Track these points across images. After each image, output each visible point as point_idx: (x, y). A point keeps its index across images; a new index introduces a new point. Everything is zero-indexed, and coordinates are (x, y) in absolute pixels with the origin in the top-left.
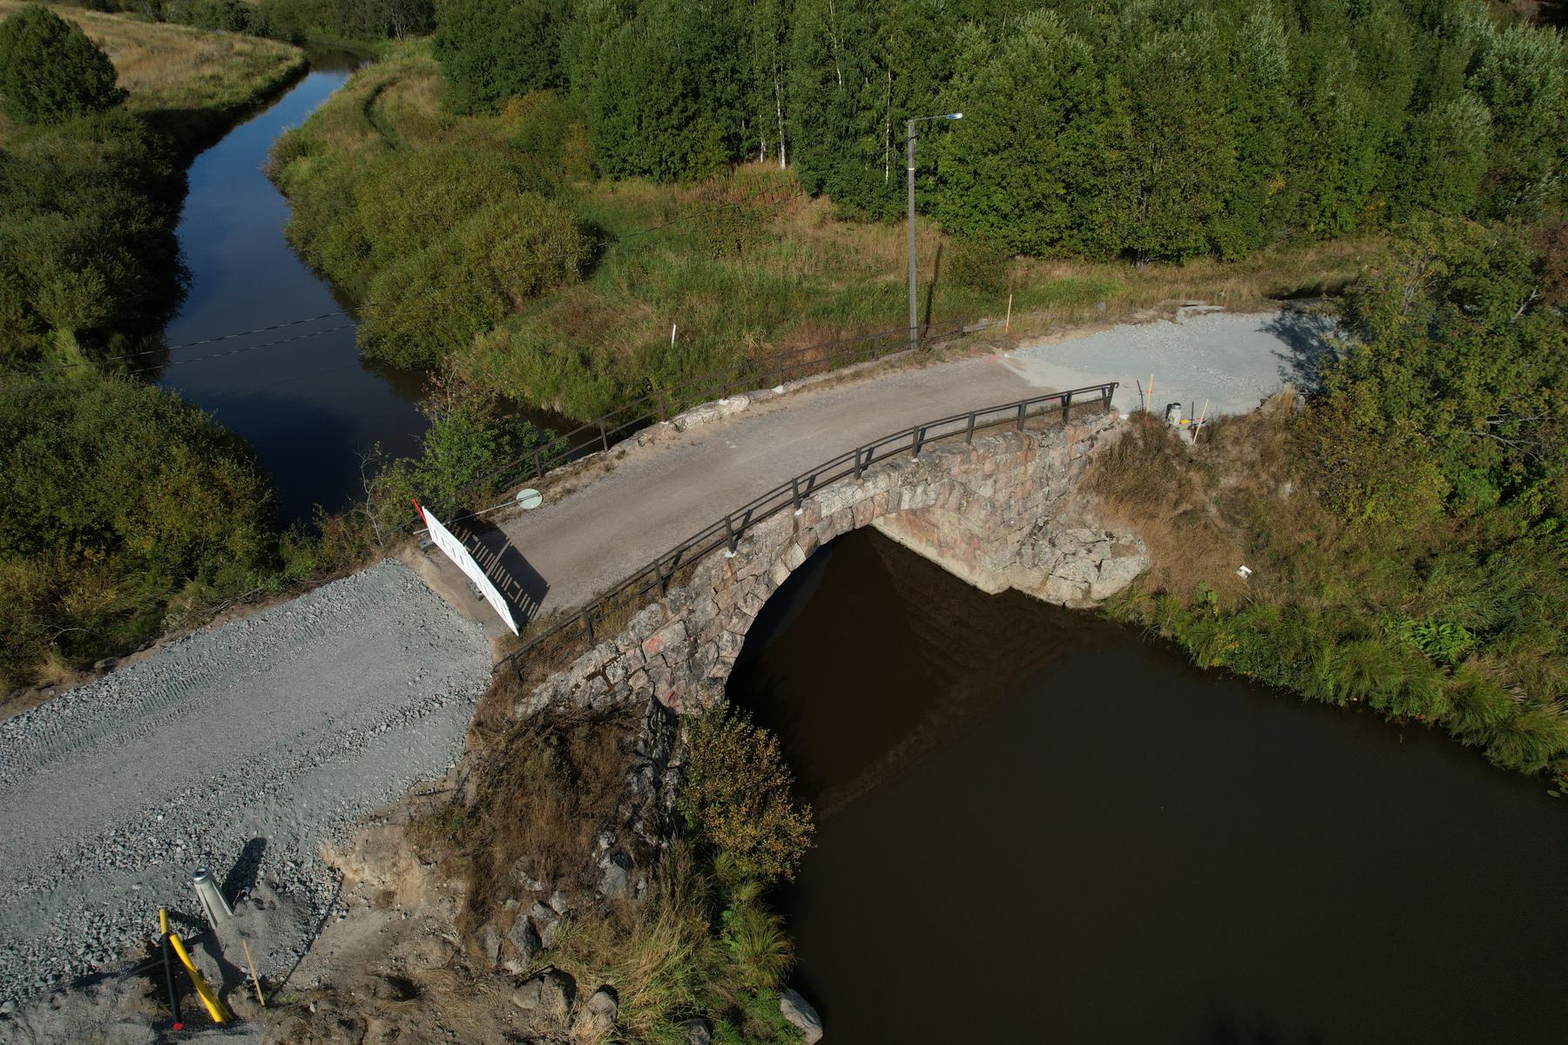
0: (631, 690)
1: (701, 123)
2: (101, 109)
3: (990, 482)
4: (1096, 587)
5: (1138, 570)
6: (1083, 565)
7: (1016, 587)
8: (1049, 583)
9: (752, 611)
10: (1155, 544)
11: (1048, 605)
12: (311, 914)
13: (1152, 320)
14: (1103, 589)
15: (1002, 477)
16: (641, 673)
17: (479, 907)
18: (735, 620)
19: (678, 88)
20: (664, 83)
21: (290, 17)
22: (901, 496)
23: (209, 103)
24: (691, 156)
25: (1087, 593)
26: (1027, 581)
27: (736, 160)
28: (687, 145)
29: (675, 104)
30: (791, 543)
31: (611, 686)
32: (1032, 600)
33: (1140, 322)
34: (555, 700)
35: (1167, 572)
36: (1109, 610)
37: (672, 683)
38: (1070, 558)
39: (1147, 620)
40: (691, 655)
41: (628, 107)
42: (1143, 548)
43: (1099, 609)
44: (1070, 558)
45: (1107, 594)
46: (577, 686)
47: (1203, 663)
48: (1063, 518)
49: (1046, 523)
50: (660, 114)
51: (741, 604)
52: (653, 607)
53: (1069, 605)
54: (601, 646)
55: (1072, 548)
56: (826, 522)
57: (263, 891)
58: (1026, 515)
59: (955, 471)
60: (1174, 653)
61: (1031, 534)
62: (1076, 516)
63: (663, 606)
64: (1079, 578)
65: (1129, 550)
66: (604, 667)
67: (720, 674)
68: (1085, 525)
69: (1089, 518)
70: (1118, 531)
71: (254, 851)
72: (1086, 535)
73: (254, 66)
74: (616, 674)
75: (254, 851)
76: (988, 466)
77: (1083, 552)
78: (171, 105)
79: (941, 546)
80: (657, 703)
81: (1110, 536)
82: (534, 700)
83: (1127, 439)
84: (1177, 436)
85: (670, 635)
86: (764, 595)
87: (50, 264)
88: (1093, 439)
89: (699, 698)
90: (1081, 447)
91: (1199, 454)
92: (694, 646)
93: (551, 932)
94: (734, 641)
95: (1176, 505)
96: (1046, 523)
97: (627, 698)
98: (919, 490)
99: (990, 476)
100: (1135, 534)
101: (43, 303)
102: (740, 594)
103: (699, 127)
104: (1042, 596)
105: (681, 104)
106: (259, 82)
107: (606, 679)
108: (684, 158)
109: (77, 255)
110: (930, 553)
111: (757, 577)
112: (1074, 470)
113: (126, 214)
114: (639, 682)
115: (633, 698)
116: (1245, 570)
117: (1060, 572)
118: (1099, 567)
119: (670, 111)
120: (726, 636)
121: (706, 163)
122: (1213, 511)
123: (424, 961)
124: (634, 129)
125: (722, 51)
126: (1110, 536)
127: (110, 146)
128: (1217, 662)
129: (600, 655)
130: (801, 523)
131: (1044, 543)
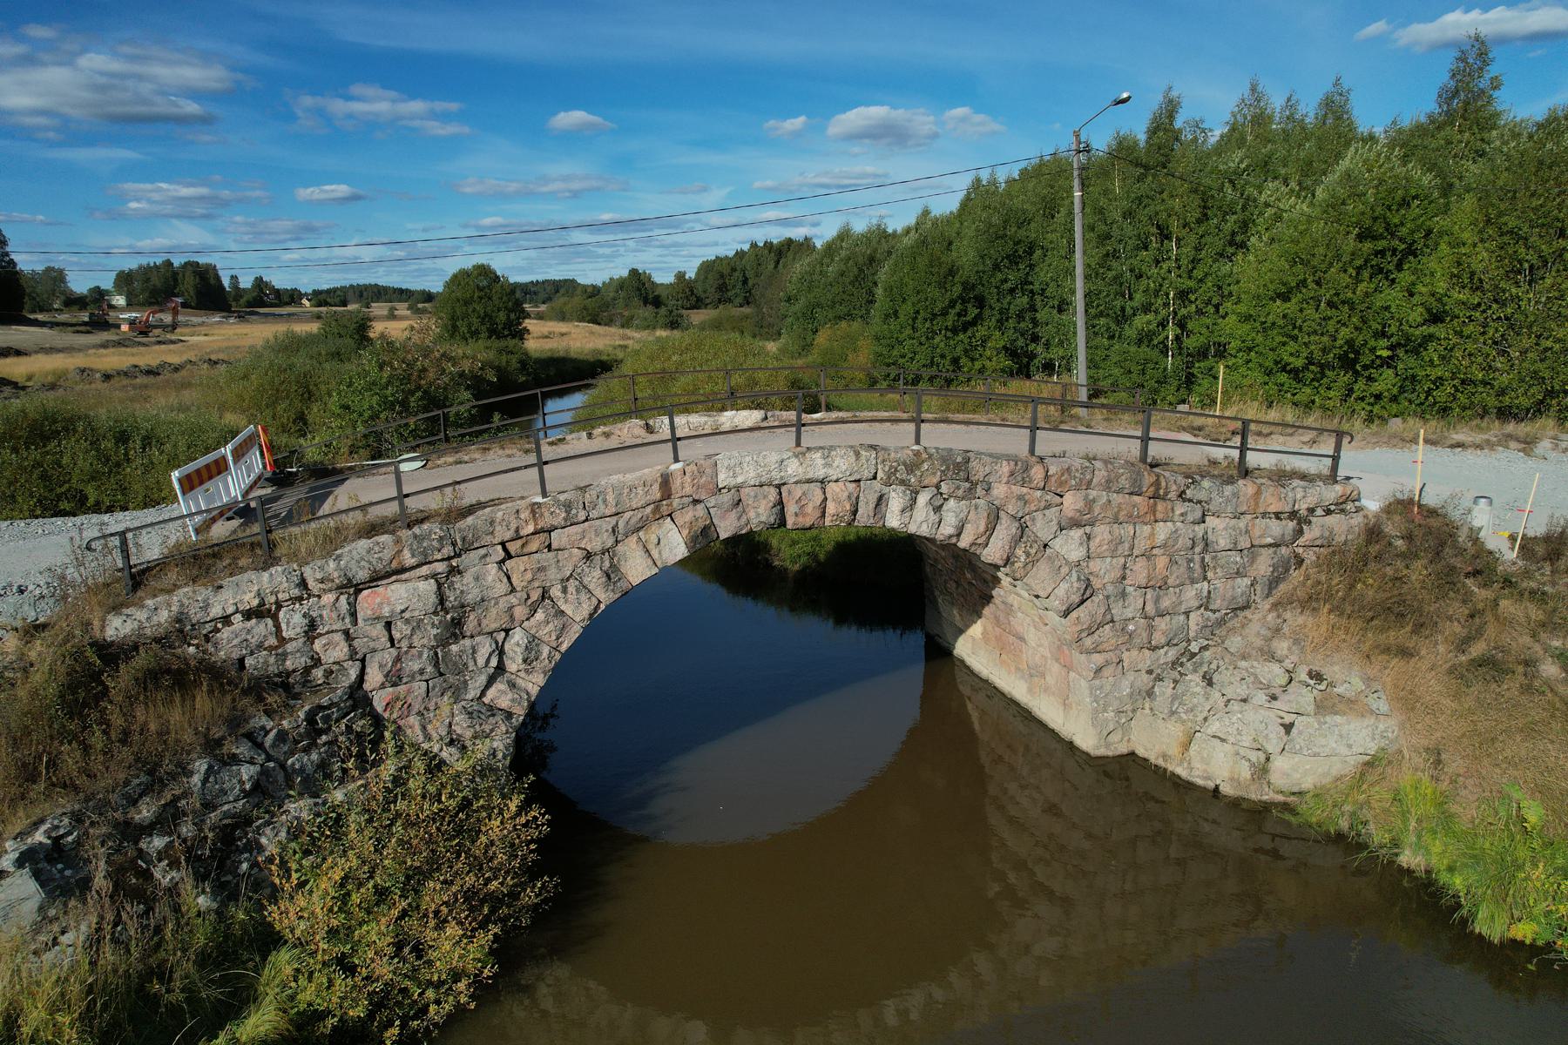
0: (317, 662)
1: (981, 331)
3: (1077, 534)
4: (1279, 764)
5: (1372, 748)
6: (1259, 721)
7: (1141, 752)
8: (1194, 747)
9: (578, 611)
10: (1407, 701)
11: (1189, 786)
13: (1490, 445)
15: (1102, 532)
16: (338, 637)
18: (540, 615)
20: (942, 285)
22: (881, 500)
24: (963, 361)
25: (1262, 771)
26: (1154, 739)
27: (1024, 372)
29: (952, 304)
30: (658, 515)
31: (283, 641)
32: (1160, 774)
33: (1460, 445)
34: (181, 630)
36: (1303, 808)
37: (394, 678)
38: (1235, 706)
39: (1377, 835)
40: (443, 642)
41: (906, 310)
42: (1384, 707)
43: (1286, 807)
44: (1235, 706)
45: (1307, 784)
46: (226, 620)
47: (1491, 924)
48: (1235, 643)
49: (1204, 648)
50: (934, 316)
51: (556, 592)
52: (385, 538)
53: (1226, 789)
54: (277, 570)
55: (1242, 691)
56: (726, 498)
58: (1162, 624)
59: (999, 490)
60: (1428, 907)
61: (1175, 664)
62: (1259, 642)
63: (398, 541)
64: (1246, 741)
65: (1350, 705)
66: (279, 606)
67: (504, 703)
68: (1272, 657)
69: (1282, 647)
70: (1333, 671)
72: (1274, 673)
74: (293, 621)
77: (1261, 698)
78: (573, 355)
79: (1034, 674)
80: (358, 697)
81: (1317, 676)
82: (141, 615)
83: (1373, 533)
84: (1476, 541)
85: (409, 595)
86: (606, 597)
88: (1301, 520)
89: (460, 727)
90: (1277, 529)
91: (1527, 574)
92: (455, 629)
94: (550, 658)
95: (1463, 644)
96: (1204, 648)
97: (307, 670)
98: (923, 499)
99: (1076, 524)
100: (1368, 680)
102: (553, 575)
103: (978, 335)
104: (1181, 771)
105: (958, 307)
107: (278, 626)
108: (955, 361)
110: (1017, 688)
111: (589, 556)
112: (1263, 566)
114: (333, 651)
115: (318, 673)
117: (1214, 727)
118: (1288, 728)
119: (944, 313)
120: (518, 636)
121: (981, 371)
124: (909, 331)
125: (1013, 259)
126: (1317, 676)
128: (1525, 931)
129: (273, 581)
130: (676, 484)
131: (1194, 681)
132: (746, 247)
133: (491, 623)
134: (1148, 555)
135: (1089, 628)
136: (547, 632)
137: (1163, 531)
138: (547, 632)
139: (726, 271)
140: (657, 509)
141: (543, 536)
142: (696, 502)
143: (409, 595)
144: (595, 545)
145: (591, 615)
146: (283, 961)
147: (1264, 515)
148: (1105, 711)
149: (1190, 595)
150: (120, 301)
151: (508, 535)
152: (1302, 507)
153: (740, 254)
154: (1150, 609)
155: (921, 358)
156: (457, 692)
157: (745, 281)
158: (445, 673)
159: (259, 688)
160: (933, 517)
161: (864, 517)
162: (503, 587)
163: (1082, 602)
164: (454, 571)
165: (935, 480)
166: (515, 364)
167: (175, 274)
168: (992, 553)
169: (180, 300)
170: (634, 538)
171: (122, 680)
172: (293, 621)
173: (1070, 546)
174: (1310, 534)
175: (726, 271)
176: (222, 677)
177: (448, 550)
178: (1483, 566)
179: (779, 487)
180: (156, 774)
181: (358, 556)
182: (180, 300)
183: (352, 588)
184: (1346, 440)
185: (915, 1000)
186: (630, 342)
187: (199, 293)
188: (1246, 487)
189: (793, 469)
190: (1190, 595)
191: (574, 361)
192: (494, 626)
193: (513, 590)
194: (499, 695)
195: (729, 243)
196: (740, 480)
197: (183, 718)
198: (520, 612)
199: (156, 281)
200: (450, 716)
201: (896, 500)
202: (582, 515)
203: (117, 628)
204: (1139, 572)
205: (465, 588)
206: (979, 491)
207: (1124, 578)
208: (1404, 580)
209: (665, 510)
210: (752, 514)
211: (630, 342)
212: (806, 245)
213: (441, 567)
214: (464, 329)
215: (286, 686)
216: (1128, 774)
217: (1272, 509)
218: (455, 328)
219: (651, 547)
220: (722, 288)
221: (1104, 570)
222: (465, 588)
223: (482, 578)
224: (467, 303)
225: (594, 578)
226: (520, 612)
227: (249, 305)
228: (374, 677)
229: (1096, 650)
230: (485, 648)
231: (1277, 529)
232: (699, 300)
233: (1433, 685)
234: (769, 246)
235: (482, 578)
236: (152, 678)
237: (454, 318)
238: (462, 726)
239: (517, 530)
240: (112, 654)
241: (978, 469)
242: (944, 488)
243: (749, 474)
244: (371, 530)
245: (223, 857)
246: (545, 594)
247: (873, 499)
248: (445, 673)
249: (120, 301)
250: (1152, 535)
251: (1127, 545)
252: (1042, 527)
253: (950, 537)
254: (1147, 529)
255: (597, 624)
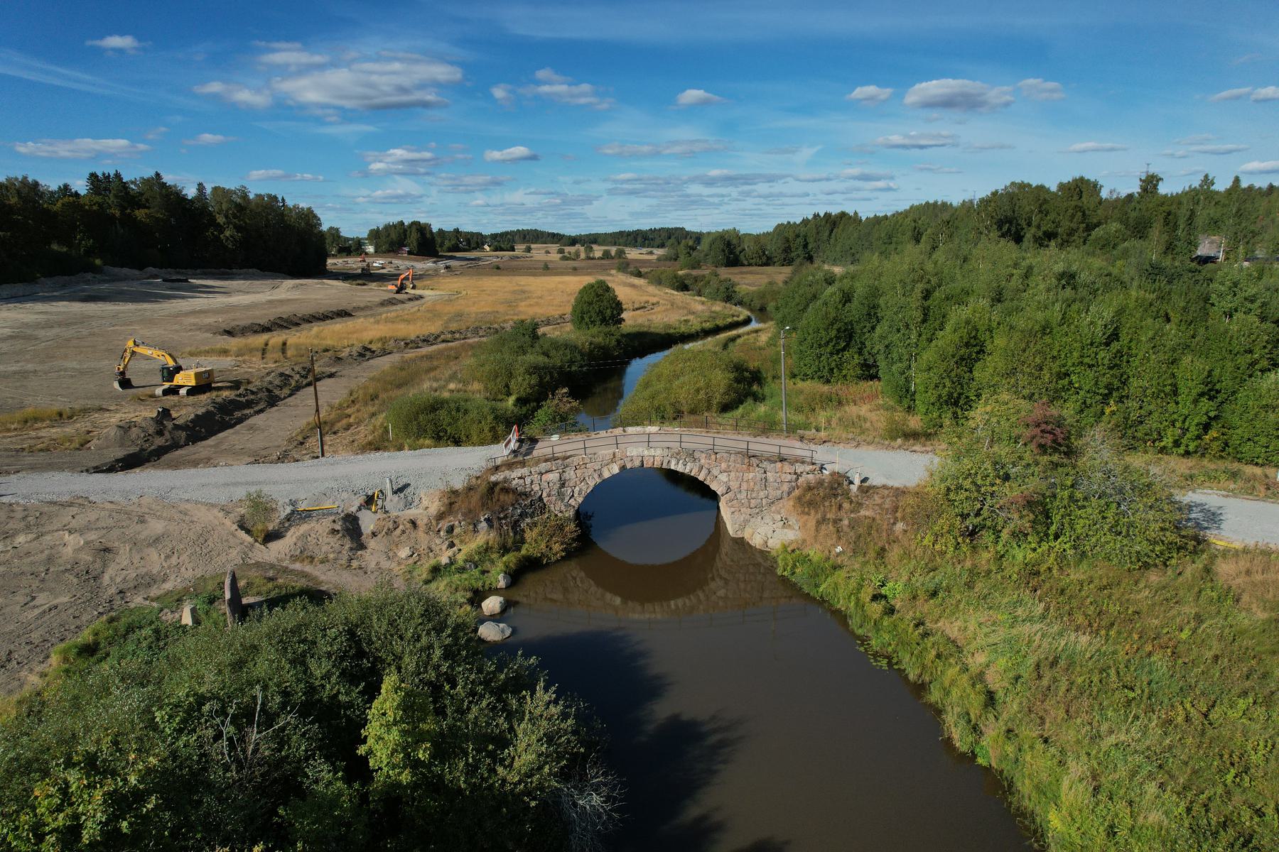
2: (607, 324)
9: (592, 484)
10: (803, 527)
12: (408, 505)
14: (775, 544)
15: (733, 474)
17: (440, 517)
19: (833, 333)
20: (826, 330)
21: (762, 295)
23: (672, 331)
28: (833, 364)
29: (831, 340)
34: (506, 480)
35: (804, 541)
37: (549, 495)
57: (402, 495)
71: (407, 486)
73: (714, 316)
74: (528, 481)
75: (407, 486)
76: (724, 465)
78: (652, 330)
80: (541, 499)
83: (820, 483)
85: (553, 476)
86: (599, 481)
87: (522, 370)
88: (798, 475)
89: (563, 509)
90: (789, 477)
92: (563, 485)
93: (457, 531)
101: (513, 385)
106: (707, 325)
108: (832, 370)
109: (534, 369)
112: (786, 487)
113: (572, 362)
114: (536, 488)
116: (839, 549)
122: (846, 522)
123: (421, 523)
127: (599, 340)
129: (525, 471)
132: (810, 217)
134: (748, 481)
136: (584, 488)
137: (751, 475)
138: (584, 488)
139: (791, 236)
143: (553, 476)
146: (526, 546)
149: (762, 494)
150: (371, 249)
152: (799, 471)
153: (805, 222)
155: (814, 368)
156: (562, 500)
157: (806, 246)
158: (560, 495)
159: (521, 494)
161: (665, 466)
166: (614, 343)
167: (405, 231)
168: (701, 478)
169: (407, 249)
171: (497, 489)
172: (528, 481)
173: (723, 477)
174: (801, 480)
175: (791, 236)
176: (514, 491)
178: (846, 494)
180: (503, 509)
181: (543, 466)
182: (407, 249)
183: (542, 474)
185: (680, 602)
186: (691, 317)
187: (420, 245)
188: (779, 465)
189: (646, 453)
190: (762, 494)
194: (572, 502)
195: (797, 213)
197: (509, 498)
199: (394, 236)
200: (560, 506)
203: (493, 478)
204: (744, 486)
205: (566, 476)
208: (826, 495)
211: (691, 317)
212: (855, 219)
214: (587, 320)
215: (526, 495)
216: (741, 543)
218: (583, 318)
220: (787, 250)
221: (734, 485)
222: (566, 476)
223: (570, 474)
224: (590, 304)
225: (596, 476)
227: (450, 250)
228: (544, 495)
231: (789, 477)
232: (769, 258)
233: (811, 521)
234: (827, 215)
235: (570, 474)
236: (502, 489)
237: (583, 313)
238: (563, 508)
240: (496, 484)
241: (697, 455)
243: (634, 453)
244: (546, 461)
245: (515, 525)
248: (560, 495)
249: (371, 249)
252: (715, 472)
255: (596, 487)
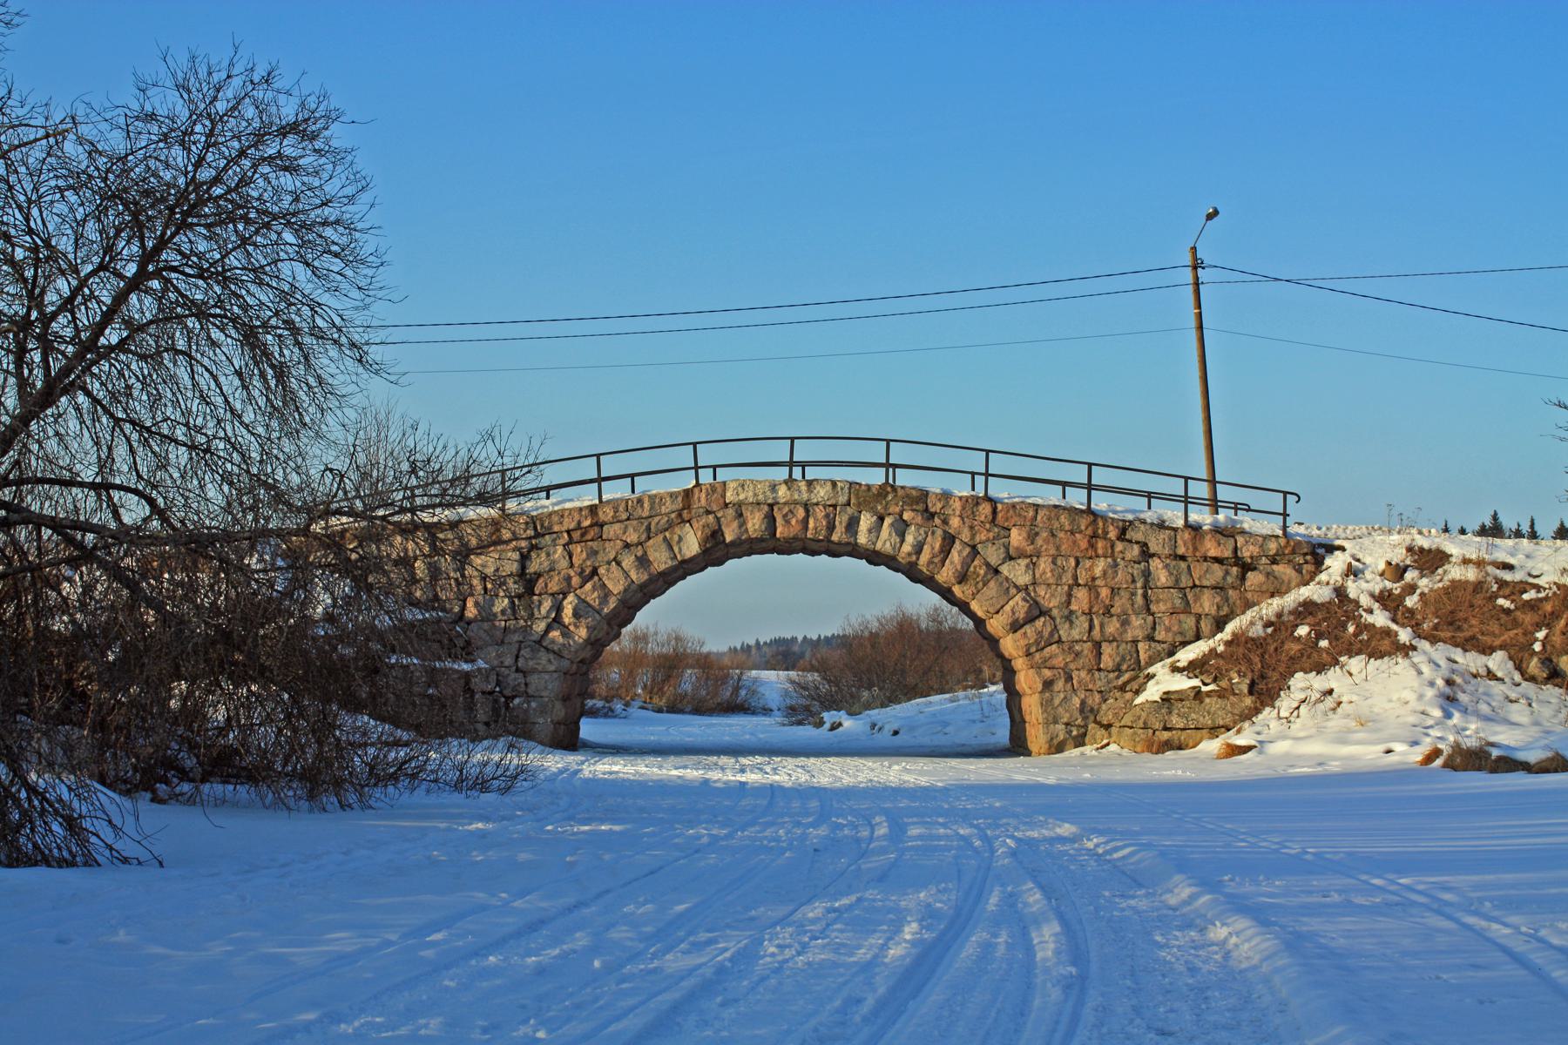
3: (1023, 562)
18: (589, 586)
22: (853, 525)
51: (602, 571)
98: (888, 521)
111: (627, 546)
120: (571, 597)
133: (554, 586)
135: (1037, 642)
138: (593, 598)
140: (680, 515)
141: (596, 529)
142: (708, 512)
144: (632, 537)
145: (625, 590)
147: (1205, 559)
148: (1056, 722)
151: (572, 526)
154: (1096, 633)
160: (896, 539)
162: (564, 563)
163: (1030, 620)
164: (533, 547)
165: (897, 509)
170: (661, 537)
173: (1017, 573)
177: (530, 532)
179: (771, 506)
184: (1291, 499)
191: (874, 636)
192: (555, 589)
193: (572, 566)
196: (742, 497)
198: (576, 581)
201: (866, 521)
202: (624, 516)
206: (937, 521)
207: (1069, 603)
209: (685, 514)
210: (749, 525)
213: (524, 544)
217: (1212, 553)
219: (674, 543)
221: (1050, 599)
225: (628, 561)
226: (576, 581)
229: (1045, 664)
230: (547, 604)
239: (579, 522)
242: (906, 516)
246: (595, 572)
247: (845, 518)
250: (1090, 569)
251: (1069, 575)
253: (909, 554)
254: (1088, 563)
